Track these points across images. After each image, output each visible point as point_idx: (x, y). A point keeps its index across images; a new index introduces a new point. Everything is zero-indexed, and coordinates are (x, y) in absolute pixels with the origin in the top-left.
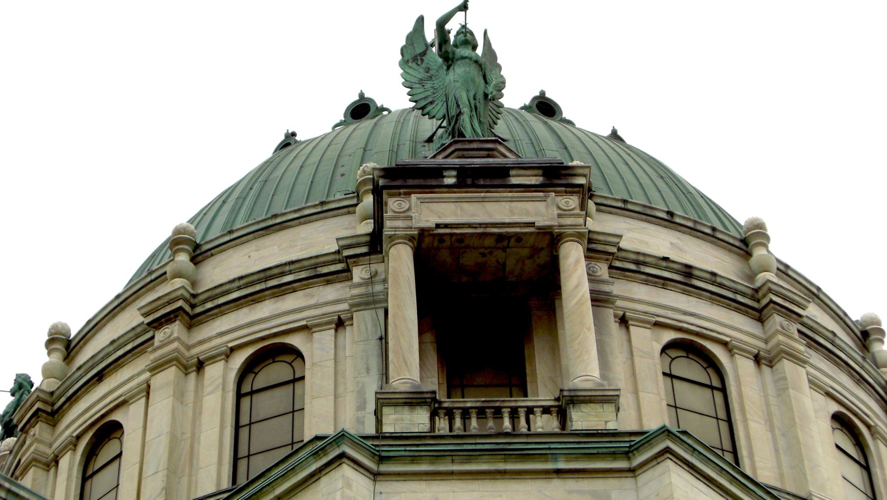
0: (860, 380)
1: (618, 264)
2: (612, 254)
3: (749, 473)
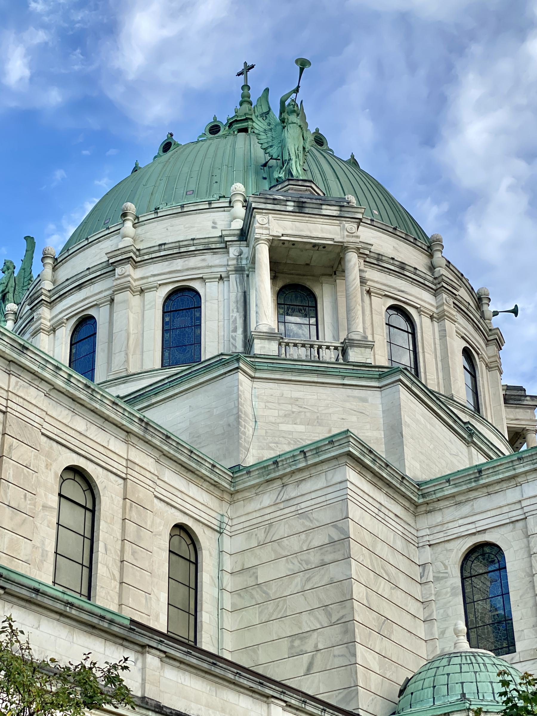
0: (477, 328)
1: (368, 260)
2: (367, 255)
3: (423, 382)
